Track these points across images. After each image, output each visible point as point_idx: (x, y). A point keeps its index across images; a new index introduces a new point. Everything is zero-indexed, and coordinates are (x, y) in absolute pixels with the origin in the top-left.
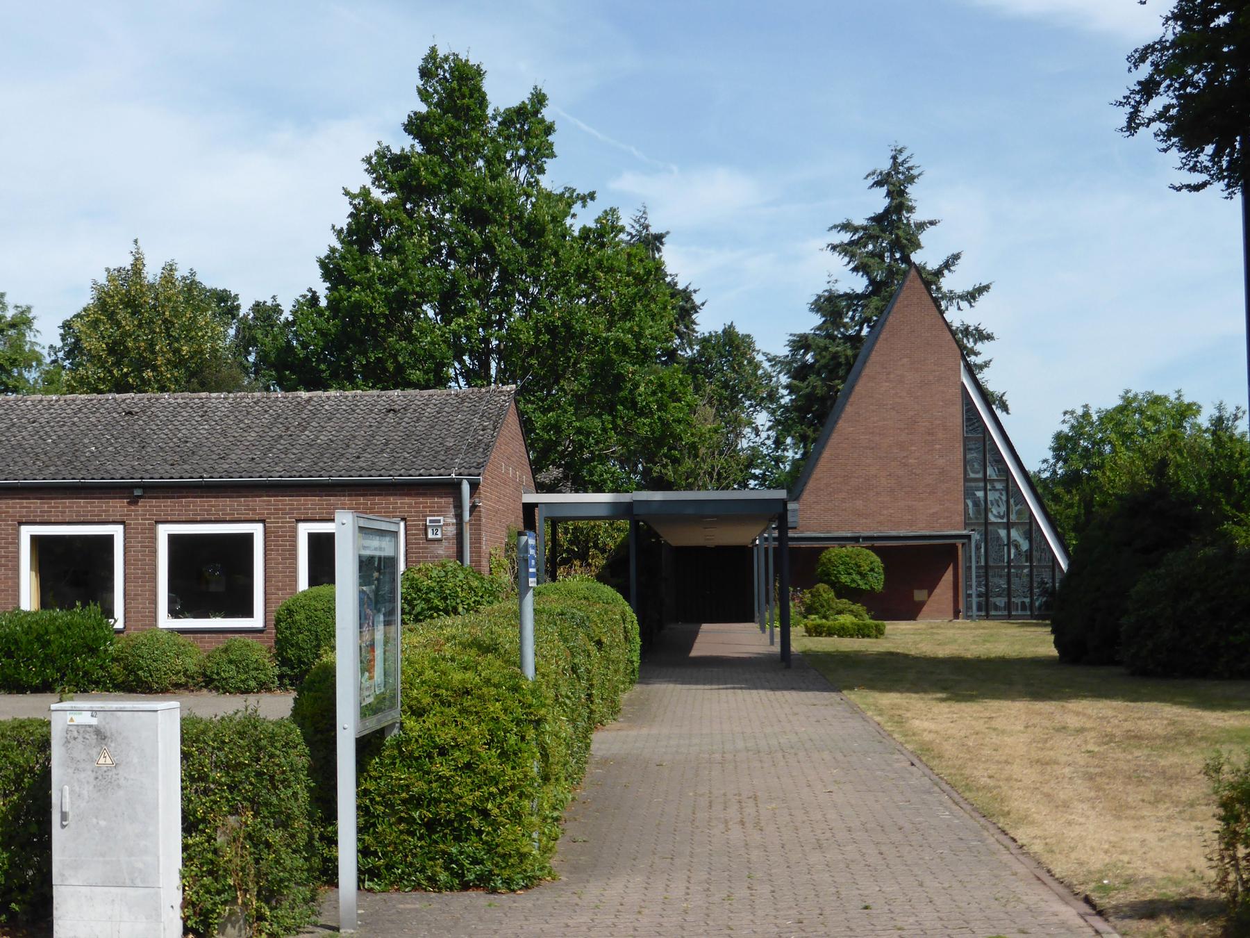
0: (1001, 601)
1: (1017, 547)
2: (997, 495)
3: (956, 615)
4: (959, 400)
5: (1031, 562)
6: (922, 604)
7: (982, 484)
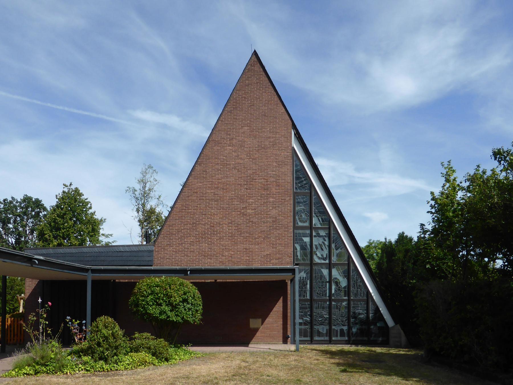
0: (323, 329)
1: (337, 283)
2: (321, 240)
4: (290, 161)
5: (349, 296)
6: (256, 330)
7: (308, 232)
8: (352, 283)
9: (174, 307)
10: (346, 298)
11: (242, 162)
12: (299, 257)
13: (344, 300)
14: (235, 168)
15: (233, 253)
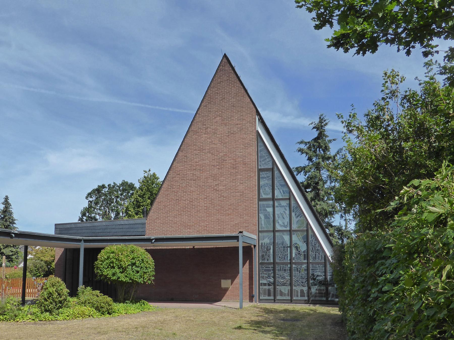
0: (285, 289)
2: (282, 210)
3: (251, 298)
5: (308, 259)
6: (226, 290)
8: (310, 247)
9: (124, 270)
10: (306, 261)
11: (215, 146)
12: (263, 225)
13: (304, 263)
14: (209, 152)
15: (207, 223)
